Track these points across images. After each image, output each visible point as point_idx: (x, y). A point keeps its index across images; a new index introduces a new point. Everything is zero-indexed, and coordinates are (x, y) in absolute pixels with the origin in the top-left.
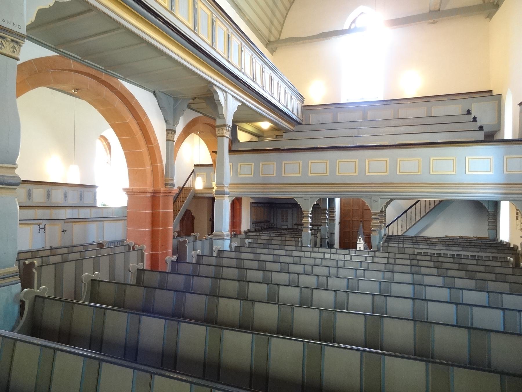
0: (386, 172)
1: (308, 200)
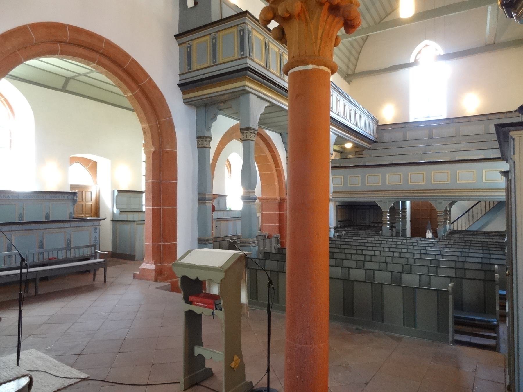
0: (448, 181)
1: (386, 202)
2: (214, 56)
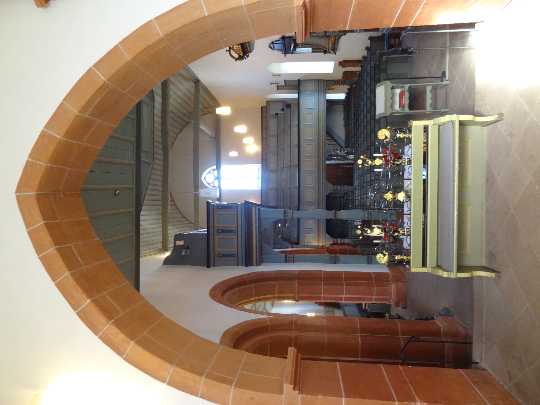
1: (327, 187)
2: (230, 231)
